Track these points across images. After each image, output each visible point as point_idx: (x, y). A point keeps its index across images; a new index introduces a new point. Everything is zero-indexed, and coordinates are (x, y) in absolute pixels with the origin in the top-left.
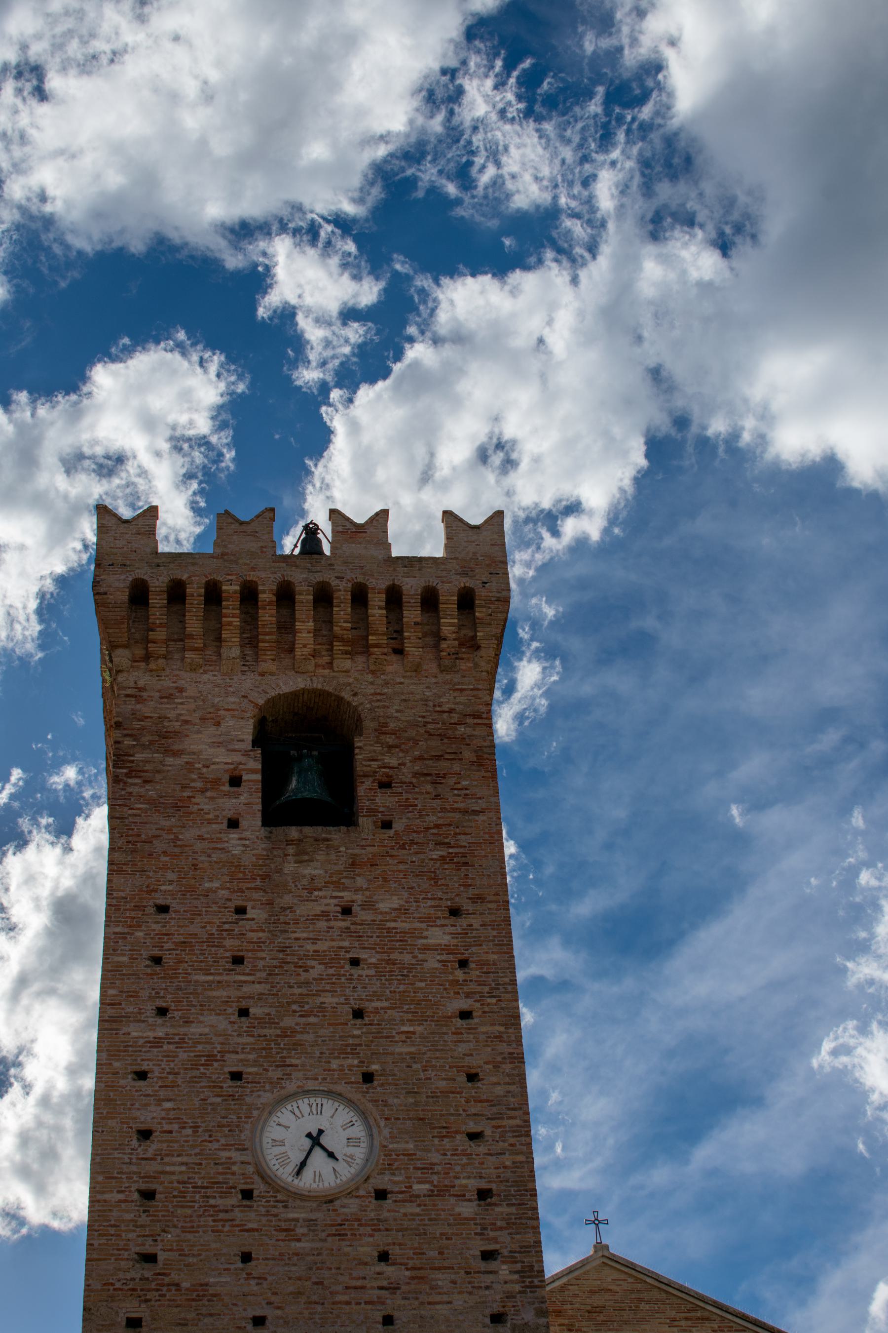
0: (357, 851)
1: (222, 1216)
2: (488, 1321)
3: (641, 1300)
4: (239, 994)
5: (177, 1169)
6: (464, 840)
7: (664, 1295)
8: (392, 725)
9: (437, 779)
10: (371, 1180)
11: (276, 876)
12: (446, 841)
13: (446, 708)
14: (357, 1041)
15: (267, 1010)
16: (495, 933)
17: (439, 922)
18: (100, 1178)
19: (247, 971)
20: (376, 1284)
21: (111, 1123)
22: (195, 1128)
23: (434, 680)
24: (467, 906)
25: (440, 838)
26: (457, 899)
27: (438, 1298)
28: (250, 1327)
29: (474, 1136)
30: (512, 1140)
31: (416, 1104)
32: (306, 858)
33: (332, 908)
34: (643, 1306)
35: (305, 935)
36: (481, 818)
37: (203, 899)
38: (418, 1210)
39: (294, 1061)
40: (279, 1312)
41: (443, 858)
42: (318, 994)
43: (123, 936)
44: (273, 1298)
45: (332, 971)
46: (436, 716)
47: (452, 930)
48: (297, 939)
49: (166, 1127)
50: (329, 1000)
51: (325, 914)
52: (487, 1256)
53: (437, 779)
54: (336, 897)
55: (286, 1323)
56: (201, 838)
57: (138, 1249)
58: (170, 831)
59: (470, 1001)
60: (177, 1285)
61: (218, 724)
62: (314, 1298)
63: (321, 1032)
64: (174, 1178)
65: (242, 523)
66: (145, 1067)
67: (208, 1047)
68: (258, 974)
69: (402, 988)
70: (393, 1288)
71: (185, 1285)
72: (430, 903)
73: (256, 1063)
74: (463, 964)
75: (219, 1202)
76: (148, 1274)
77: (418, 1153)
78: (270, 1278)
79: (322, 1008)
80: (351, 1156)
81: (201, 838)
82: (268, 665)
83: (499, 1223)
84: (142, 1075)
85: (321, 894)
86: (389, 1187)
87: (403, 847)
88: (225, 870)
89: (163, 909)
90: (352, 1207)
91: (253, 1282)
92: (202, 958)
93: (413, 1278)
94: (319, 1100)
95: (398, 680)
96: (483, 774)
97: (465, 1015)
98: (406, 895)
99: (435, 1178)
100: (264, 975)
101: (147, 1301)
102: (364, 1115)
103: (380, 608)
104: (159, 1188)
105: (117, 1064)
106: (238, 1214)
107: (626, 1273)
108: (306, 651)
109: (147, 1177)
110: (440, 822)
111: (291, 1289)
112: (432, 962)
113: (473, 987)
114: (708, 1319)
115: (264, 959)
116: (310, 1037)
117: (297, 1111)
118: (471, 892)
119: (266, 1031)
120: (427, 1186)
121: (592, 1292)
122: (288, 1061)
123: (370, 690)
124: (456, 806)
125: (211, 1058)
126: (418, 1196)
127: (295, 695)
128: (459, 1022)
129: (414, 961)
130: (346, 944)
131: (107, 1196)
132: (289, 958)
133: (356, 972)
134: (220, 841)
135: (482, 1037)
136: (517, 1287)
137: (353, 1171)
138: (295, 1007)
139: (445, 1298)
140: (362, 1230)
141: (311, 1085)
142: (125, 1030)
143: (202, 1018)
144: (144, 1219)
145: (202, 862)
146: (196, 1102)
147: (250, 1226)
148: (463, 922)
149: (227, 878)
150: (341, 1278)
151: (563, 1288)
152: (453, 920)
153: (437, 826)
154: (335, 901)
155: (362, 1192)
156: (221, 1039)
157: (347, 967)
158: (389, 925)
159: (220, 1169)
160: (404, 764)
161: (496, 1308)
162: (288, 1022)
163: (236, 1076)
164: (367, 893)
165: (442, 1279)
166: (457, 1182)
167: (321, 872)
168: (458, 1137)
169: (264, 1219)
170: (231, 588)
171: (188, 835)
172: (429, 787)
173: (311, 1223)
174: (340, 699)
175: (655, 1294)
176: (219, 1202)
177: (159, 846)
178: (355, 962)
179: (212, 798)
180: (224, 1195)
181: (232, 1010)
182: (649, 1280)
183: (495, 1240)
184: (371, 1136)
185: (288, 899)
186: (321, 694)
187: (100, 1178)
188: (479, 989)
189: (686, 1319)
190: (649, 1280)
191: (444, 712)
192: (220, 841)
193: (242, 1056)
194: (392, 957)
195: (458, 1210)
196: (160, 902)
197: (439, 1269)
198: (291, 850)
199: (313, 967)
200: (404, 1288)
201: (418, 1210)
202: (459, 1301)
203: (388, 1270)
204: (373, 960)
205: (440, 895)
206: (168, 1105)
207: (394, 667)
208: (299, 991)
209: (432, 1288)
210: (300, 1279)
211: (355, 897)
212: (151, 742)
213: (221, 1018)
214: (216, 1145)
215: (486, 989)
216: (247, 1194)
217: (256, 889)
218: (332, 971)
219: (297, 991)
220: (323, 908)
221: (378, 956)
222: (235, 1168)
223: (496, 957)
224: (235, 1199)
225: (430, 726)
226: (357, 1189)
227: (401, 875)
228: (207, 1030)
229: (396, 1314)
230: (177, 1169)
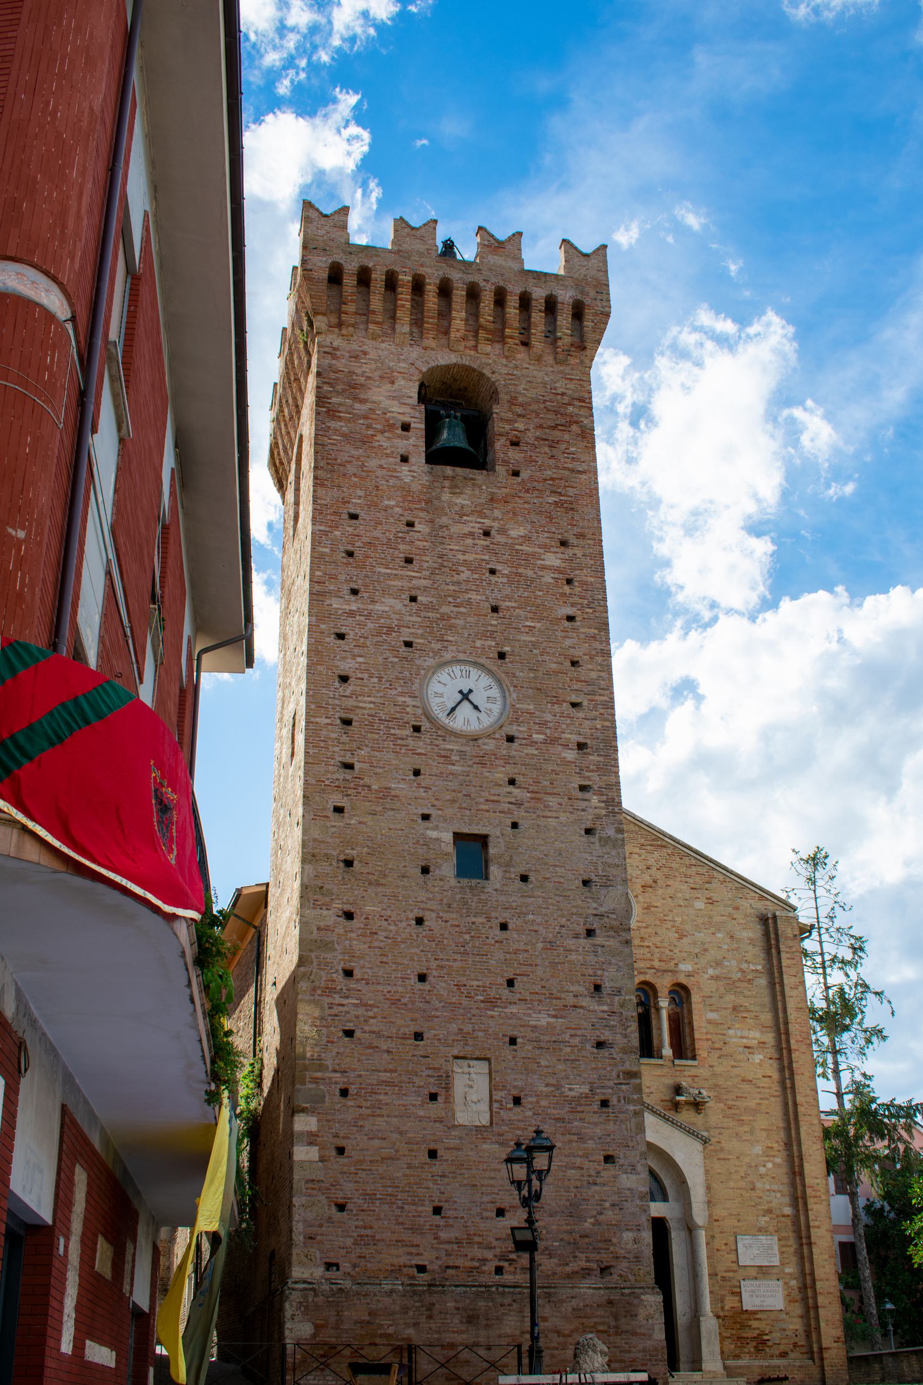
0: (495, 490)
1: (399, 742)
2: (583, 832)
4: (410, 585)
5: (368, 705)
6: (571, 491)
8: (520, 399)
9: (553, 444)
10: (504, 728)
11: (436, 502)
12: (559, 490)
13: (559, 391)
14: (494, 629)
15: (430, 599)
16: (592, 562)
17: (552, 550)
18: (313, 707)
19: (416, 569)
20: (507, 800)
21: (320, 668)
22: (380, 678)
23: (551, 369)
24: (573, 540)
25: (554, 488)
26: (566, 534)
27: (549, 814)
28: (420, 820)
29: (574, 705)
30: (602, 711)
31: (536, 678)
32: (458, 491)
33: (476, 530)
35: (457, 548)
36: (584, 477)
37: (383, 513)
38: (536, 752)
39: (450, 638)
40: (440, 812)
41: (556, 503)
42: (466, 591)
43: (326, 533)
44: (436, 803)
45: (476, 576)
46: (552, 396)
47: (562, 556)
48: (451, 550)
49: (359, 675)
50: (474, 597)
51: (471, 534)
52: (583, 788)
53: (553, 444)
54: (479, 523)
55: (445, 820)
56: (381, 467)
57: (340, 759)
58: (358, 459)
59: (574, 609)
60: (369, 786)
61: (393, 383)
62: (464, 805)
63: (469, 619)
64: (366, 712)
65: (413, 229)
66: (343, 630)
67: (388, 621)
68: (424, 573)
69: (526, 594)
70: (519, 804)
71: (374, 787)
72: (546, 535)
73: (422, 636)
74: (569, 582)
75: (397, 732)
76: (348, 777)
77: (537, 713)
78: (434, 789)
79: (469, 602)
80: (490, 710)
81: (381, 467)
82: (431, 343)
83: (592, 767)
84: (341, 636)
85: (468, 519)
86: (516, 734)
87: (527, 491)
88: (399, 493)
89: (354, 517)
90: (490, 745)
91: (422, 790)
92: (383, 556)
93: (532, 798)
94: (467, 668)
95: (525, 366)
96: (585, 444)
97: (570, 619)
98: (529, 527)
99: (548, 731)
100: (428, 573)
101: (348, 795)
102: (499, 682)
103: (515, 308)
104: (355, 718)
105: (323, 626)
106: (410, 742)
108: (458, 335)
109: (346, 709)
110: (555, 476)
111: (448, 797)
112: (548, 578)
113: (576, 599)
114: (665, 847)
115: (428, 562)
116: (460, 622)
117: (452, 674)
118: (576, 530)
119: (430, 614)
120: (542, 736)
122: (446, 638)
123: (504, 371)
124: (566, 465)
125: (390, 630)
126: (536, 743)
127: (448, 368)
128: (566, 624)
129: (534, 576)
130: (487, 557)
131: (318, 720)
132: (445, 564)
133: (493, 579)
134: (395, 470)
135: (582, 636)
136: (604, 812)
137: (491, 720)
138: (450, 599)
139: (554, 814)
140: (497, 762)
141: (461, 656)
142: (328, 602)
143: (383, 600)
144: (344, 738)
145: (382, 485)
146: (380, 659)
147: (419, 751)
148: (570, 552)
149: (401, 499)
150: (483, 794)
152: (562, 549)
153: (552, 479)
154: (479, 525)
155: (497, 736)
156: (397, 616)
157: (487, 574)
158: (517, 547)
159: (398, 709)
160: (529, 430)
161: (589, 825)
162: (445, 609)
163: (408, 644)
164: (502, 522)
165: (553, 801)
166: (563, 736)
167: (469, 503)
168: (565, 704)
169: (429, 747)
170: (405, 278)
171: (372, 463)
172: (547, 449)
173: (462, 753)
174: (482, 375)
175: (632, 827)
176: (397, 732)
177: (350, 469)
178: (493, 572)
179: (389, 438)
180: (401, 727)
181: (406, 596)
183: (589, 778)
184: (504, 697)
185: (444, 520)
186: (468, 369)
187: (313, 707)
188: (580, 601)
189: (651, 845)
190: (628, 817)
191: (558, 394)
192: (395, 470)
193: (413, 631)
194: (520, 571)
195: (563, 755)
196: (352, 511)
197: (550, 794)
198: (447, 483)
199: (463, 572)
200: (526, 805)
201: (536, 752)
202: (563, 817)
203: (516, 791)
204: (506, 572)
205: (553, 529)
206: (360, 660)
207: (522, 355)
208: (453, 588)
209: (545, 807)
210: (454, 791)
211: (493, 524)
212: (344, 390)
213: (397, 601)
214: (395, 692)
215: (586, 602)
216: (417, 729)
217: (422, 510)
218: (476, 576)
219: (451, 588)
220: (470, 530)
221: (509, 569)
222: (408, 709)
223: (592, 579)
224: (408, 731)
225: (547, 403)
226: (494, 733)
227: (526, 512)
228: (387, 609)
229: (520, 822)
230: (368, 705)
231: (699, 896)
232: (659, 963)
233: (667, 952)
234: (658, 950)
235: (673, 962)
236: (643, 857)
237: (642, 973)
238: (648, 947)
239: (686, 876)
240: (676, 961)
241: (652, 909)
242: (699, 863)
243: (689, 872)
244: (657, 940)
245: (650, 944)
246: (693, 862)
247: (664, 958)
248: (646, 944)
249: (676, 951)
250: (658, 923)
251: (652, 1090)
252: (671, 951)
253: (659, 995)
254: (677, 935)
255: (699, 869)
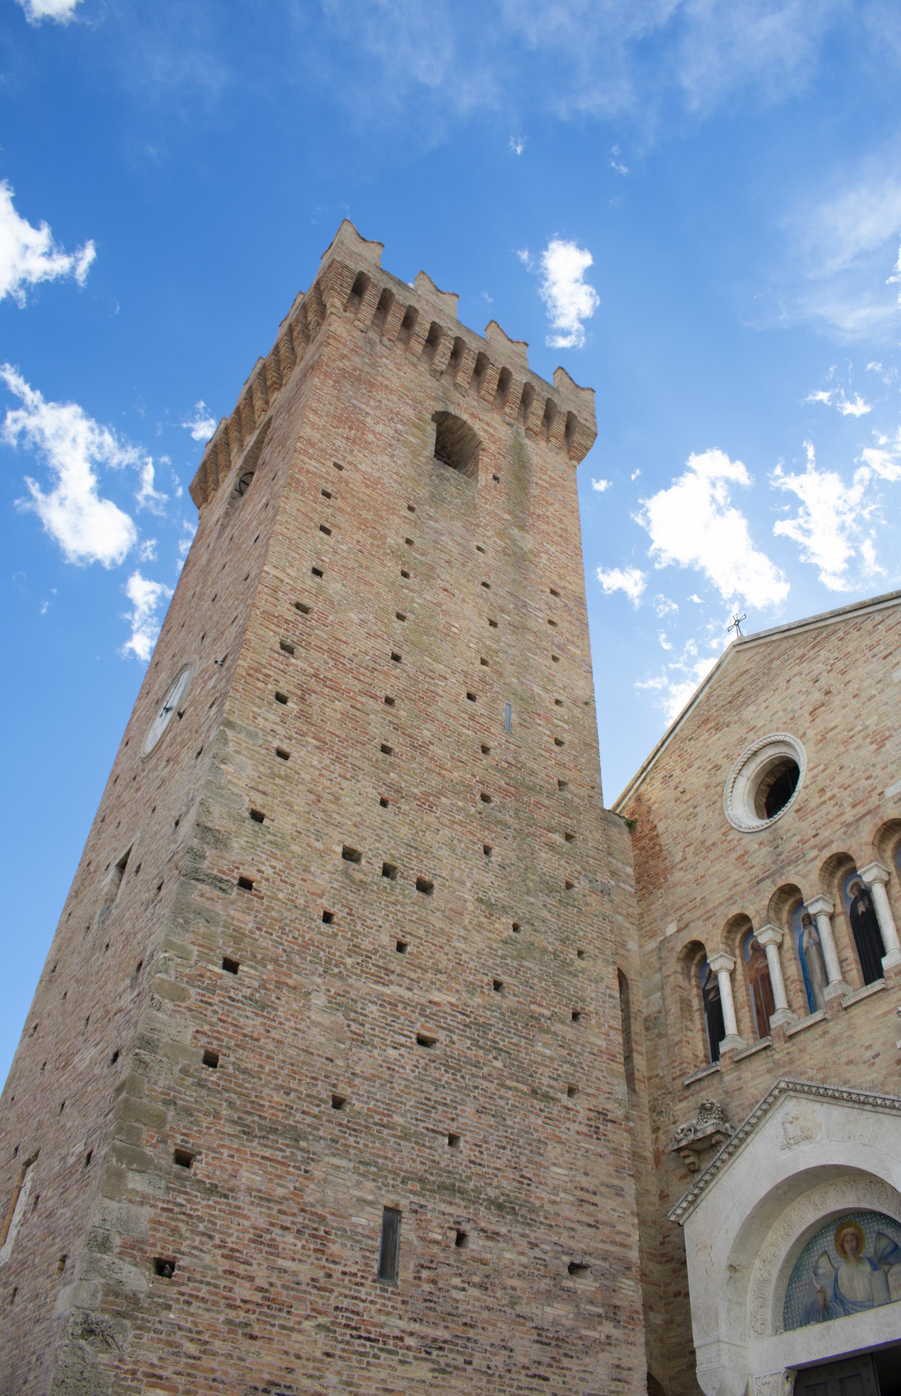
3: (771, 661)
7: (791, 641)
34: (775, 664)
107: (757, 646)
114: (834, 632)
121: (731, 684)
151: (708, 698)
175: (785, 645)
182: (774, 638)
189: (814, 647)
190: (774, 638)
231: (895, 662)
232: (854, 811)
233: (864, 783)
234: (847, 792)
235: (875, 795)
236: (805, 672)
237: (824, 847)
238: (834, 796)
239: (871, 648)
240: (879, 790)
241: (828, 736)
242: (891, 611)
243: (876, 636)
244: (843, 778)
245: (835, 791)
246: (878, 618)
247: (860, 796)
248: (829, 794)
249: (878, 772)
250: (842, 749)
251: (876, 1048)
252: (867, 778)
253: (858, 864)
254: (874, 746)
255: (887, 622)
